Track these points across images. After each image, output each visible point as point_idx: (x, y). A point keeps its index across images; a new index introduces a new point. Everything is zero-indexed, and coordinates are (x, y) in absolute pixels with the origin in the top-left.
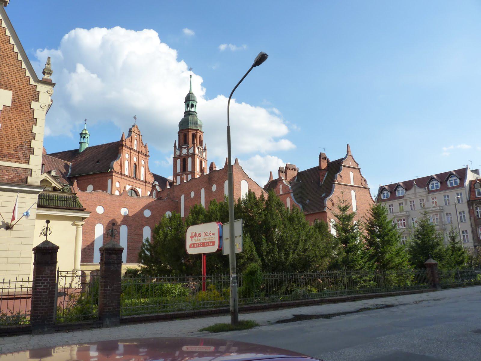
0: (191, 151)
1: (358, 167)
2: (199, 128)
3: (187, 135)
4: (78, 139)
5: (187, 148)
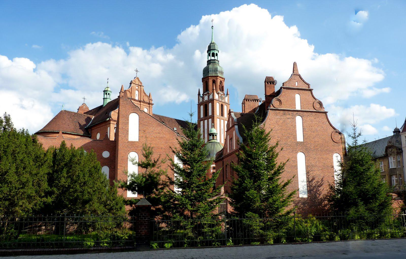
0: (211, 97)
1: (309, 87)
2: (219, 75)
3: (208, 82)
4: (102, 95)
5: (207, 95)
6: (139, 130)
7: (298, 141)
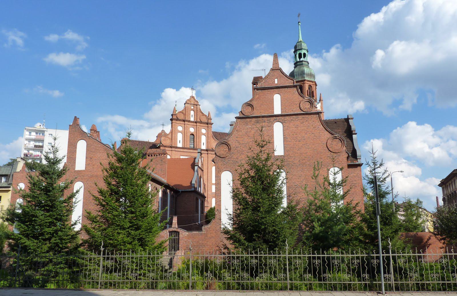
6: (86, 158)
7: (275, 155)
